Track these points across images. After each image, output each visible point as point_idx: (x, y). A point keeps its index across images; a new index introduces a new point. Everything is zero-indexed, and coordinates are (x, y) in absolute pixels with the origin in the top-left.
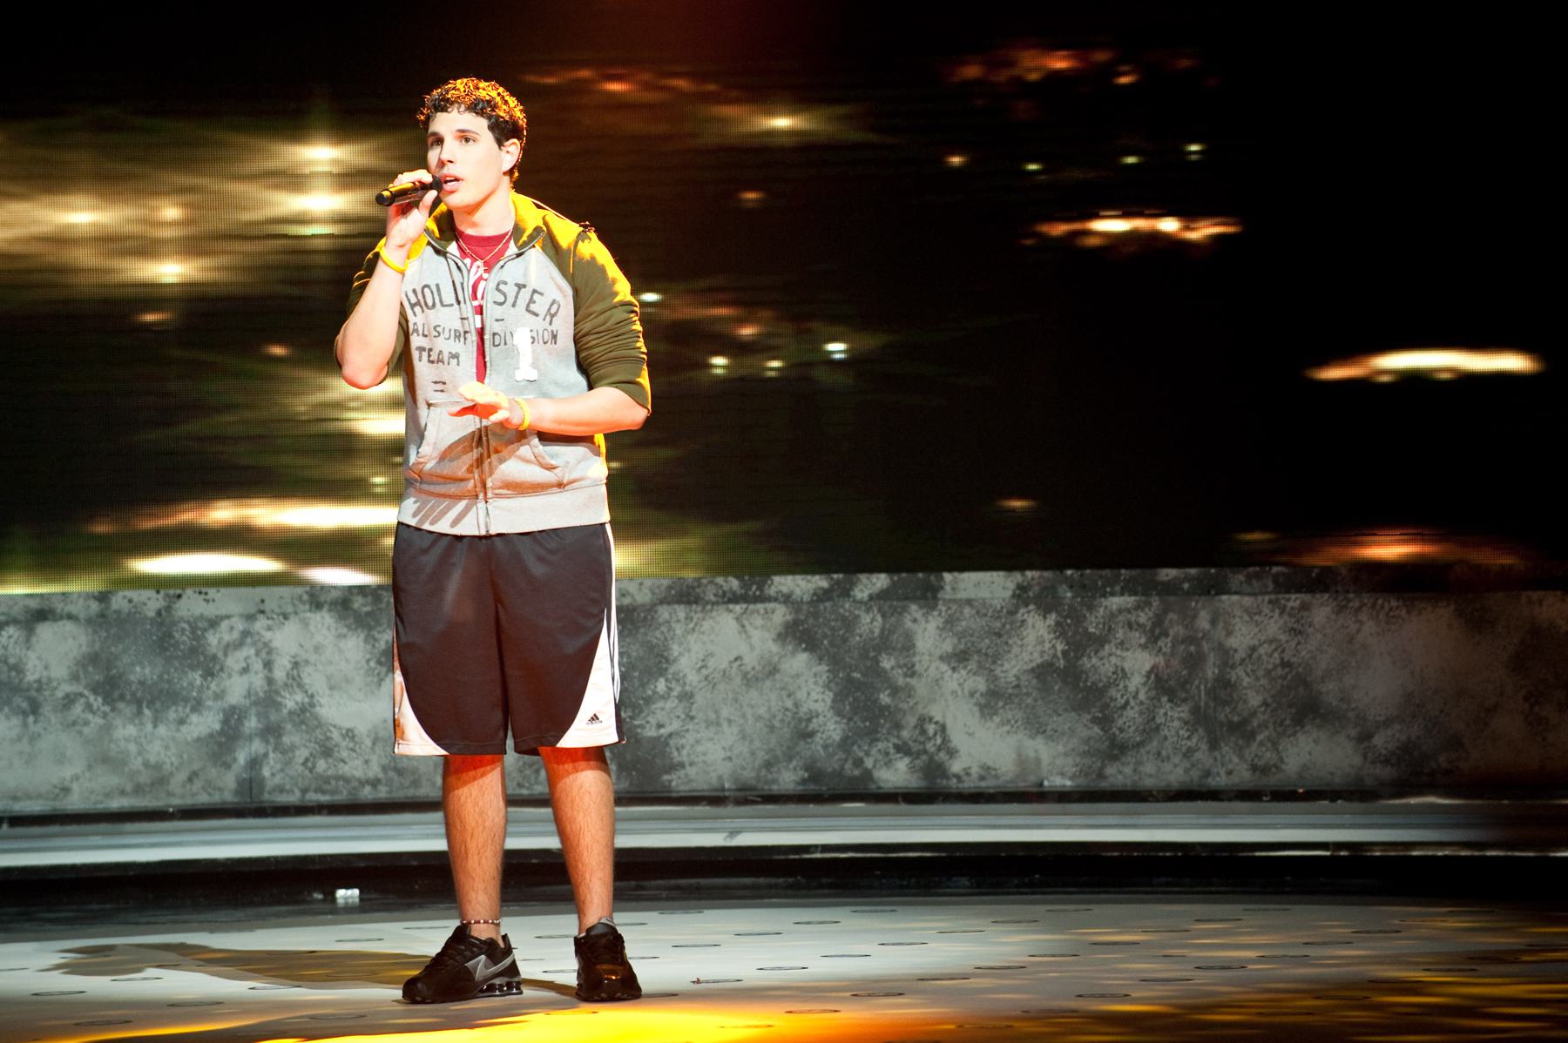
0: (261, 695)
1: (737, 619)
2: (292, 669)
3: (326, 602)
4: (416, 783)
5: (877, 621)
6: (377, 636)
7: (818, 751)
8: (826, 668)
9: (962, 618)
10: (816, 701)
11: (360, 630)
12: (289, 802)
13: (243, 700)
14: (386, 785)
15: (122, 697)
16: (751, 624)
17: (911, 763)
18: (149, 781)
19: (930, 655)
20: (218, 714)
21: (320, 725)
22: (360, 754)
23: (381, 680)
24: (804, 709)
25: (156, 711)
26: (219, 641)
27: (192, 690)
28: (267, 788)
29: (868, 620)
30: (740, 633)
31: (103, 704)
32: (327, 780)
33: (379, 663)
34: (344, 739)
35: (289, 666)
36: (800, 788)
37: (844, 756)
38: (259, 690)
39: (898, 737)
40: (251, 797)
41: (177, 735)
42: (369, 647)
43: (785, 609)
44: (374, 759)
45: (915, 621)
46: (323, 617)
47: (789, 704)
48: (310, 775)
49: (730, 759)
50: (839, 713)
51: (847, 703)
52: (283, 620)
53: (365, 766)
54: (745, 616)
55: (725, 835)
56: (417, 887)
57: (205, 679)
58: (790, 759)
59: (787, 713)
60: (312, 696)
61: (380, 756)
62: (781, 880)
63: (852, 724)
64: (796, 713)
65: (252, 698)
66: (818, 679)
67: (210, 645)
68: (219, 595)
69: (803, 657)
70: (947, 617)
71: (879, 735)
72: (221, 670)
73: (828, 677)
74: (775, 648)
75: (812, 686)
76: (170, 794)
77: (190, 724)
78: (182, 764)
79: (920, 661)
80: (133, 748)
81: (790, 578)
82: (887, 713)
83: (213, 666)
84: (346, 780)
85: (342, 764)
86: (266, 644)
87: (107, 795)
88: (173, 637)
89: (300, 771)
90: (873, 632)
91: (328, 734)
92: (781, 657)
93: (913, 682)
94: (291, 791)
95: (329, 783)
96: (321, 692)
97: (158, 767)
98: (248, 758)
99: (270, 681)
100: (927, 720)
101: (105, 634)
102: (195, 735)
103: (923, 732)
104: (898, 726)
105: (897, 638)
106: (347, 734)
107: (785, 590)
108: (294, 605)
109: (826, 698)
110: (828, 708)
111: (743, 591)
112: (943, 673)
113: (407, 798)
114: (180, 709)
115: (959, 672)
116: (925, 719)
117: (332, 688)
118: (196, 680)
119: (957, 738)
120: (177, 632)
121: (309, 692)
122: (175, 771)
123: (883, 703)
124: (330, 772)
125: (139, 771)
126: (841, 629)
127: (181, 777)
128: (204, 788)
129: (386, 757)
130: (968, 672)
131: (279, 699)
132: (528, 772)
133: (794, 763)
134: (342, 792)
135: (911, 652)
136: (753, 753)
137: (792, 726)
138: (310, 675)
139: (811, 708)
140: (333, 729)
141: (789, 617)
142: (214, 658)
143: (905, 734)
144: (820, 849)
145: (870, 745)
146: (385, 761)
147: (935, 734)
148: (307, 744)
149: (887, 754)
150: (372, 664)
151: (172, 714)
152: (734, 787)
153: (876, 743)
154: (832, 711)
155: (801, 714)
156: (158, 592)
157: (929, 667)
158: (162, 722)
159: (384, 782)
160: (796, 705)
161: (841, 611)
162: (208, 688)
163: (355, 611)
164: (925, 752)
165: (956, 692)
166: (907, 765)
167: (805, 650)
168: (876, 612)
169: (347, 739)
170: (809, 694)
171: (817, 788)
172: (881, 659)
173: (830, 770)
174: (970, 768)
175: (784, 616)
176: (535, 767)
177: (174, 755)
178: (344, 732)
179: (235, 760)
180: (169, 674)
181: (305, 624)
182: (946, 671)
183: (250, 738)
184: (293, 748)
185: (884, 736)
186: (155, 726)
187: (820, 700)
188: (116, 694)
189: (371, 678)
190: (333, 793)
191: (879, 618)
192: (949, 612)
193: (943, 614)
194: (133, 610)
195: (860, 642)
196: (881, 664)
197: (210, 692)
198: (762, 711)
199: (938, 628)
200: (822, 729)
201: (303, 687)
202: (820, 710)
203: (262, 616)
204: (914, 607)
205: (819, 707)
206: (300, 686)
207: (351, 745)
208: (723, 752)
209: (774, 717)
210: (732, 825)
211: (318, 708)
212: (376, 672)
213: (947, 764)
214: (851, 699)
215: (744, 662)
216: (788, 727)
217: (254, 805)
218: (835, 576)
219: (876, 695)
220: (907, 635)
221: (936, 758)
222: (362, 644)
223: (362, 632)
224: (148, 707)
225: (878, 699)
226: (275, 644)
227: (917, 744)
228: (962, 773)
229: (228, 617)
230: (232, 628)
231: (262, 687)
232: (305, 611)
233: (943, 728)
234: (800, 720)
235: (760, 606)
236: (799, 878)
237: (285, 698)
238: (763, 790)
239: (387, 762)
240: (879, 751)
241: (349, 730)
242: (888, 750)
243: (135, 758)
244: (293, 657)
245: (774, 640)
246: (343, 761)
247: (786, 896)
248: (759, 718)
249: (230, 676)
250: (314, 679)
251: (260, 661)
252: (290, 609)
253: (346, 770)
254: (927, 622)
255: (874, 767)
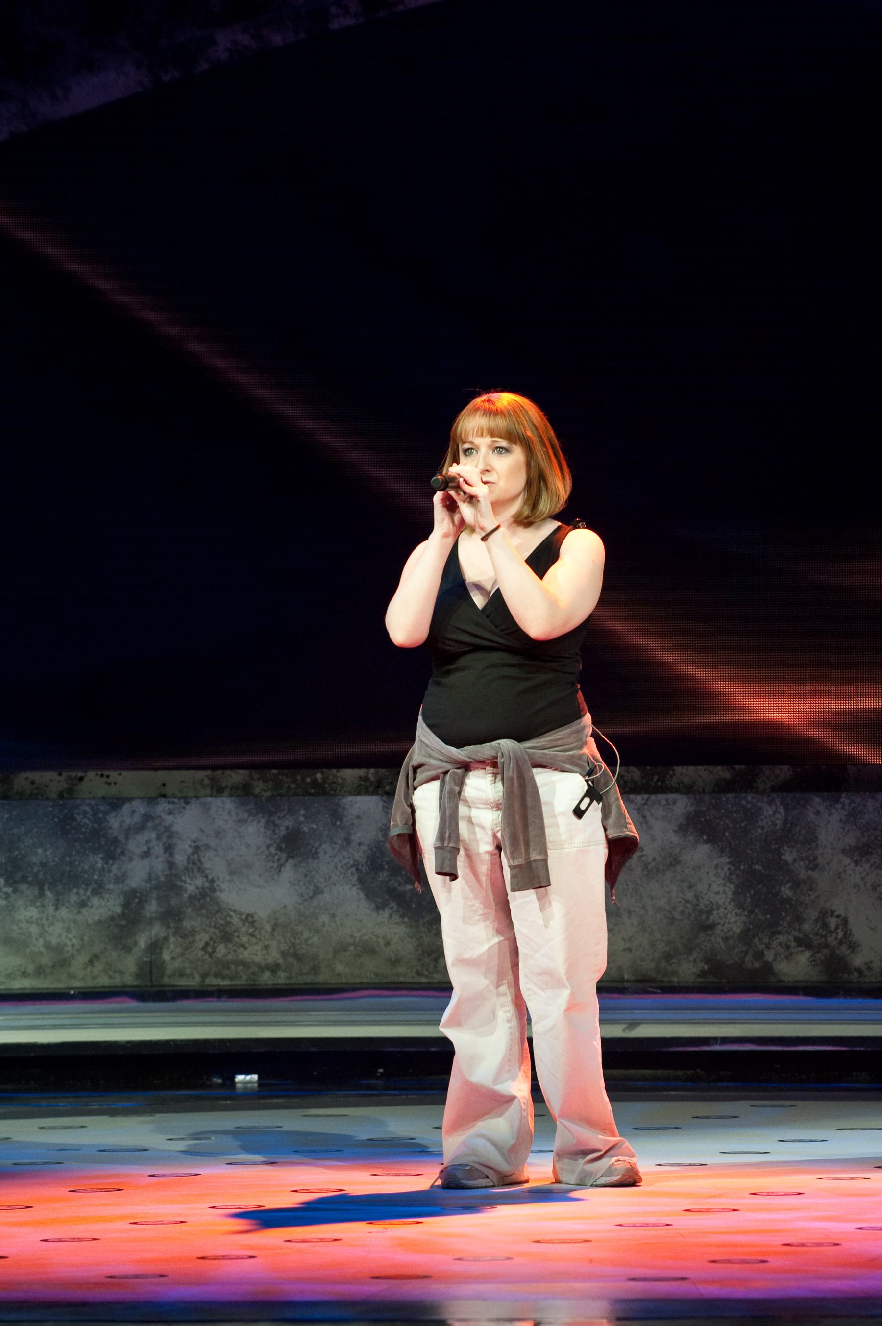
0: (162, 878)
1: (638, 809)
2: (193, 853)
3: (227, 787)
4: (315, 969)
5: (779, 813)
6: (277, 822)
7: (719, 943)
8: (728, 860)
9: (866, 811)
10: (718, 893)
11: (261, 815)
12: (188, 986)
13: (144, 884)
14: (285, 971)
15: (24, 879)
16: (652, 815)
17: (811, 956)
18: (50, 964)
19: (833, 848)
20: (119, 897)
21: (220, 910)
22: (260, 940)
23: (281, 866)
24: (704, 902)
25: (58, 894)
26: (121, 826)
27: (94, 874)
28: (168, 972)
29: (771, 813)
30: (641, 824)
31: (5, 886)
32: (227, 965)
33: (280, 849)
34: (244, 925)
35: (190, 851)
36: (701, 980)
37: (744, 949)
38: (160, 874)
39: (800, 930)
40: (151, 982)
41: (79, 917)
42: (270, 832)
43: (687, 800)
44: (275, 943)
45: (818, 813)
46: (223, 801)
47: (689, 895)
48: (209, 959)
49: (630, 950)
50: (740, 906)
51: (748, 895)
52: (184, 805)
53: (265, 952)
54: (646, 807)
55: (624, 1026)
56: (315, 1073)
57: (107, 863)
58: (690, 951)
59: (688, 905)
60: (212, 881)
61: (279, 942)
62: (680, 1073)
63: (752, 916)
64: (697, 905)
65: (153, 882)
66: (720, 871)
67: (111, 828)
68: (121, 777)
69: (704, 849)
70: (850, 810)
71: (780, 928)
72: (123, 853)
73: (729, 869)
74: (676, 839)
75: (713, 879)
76: (71, 976)
77: (92, 907)
78: (83, 946)
79: (822, 854)
80: (34, 929)
81: (692, 768)
82: (788, 906)
83: (115, 849)
84: (245, 965)
85: (242, 949)
86: (167, 829)
87: (8, 976)
88: (74, 819)
89: (200, 955)
90: (776, 825)
91: (228, 919)
92: (682, 849)
93: (815, 875)
94: (191, 975)
95: (229, 968)
96: (221, 877)
97: (59, 949)
98: (149, 942)
99: (171, 865)
100: (829, 913)
101: (7, 816)
102: (96, 918)
103: (825, 925)
104: (799, 919)
105: (800, 831)
106: (247, 918)
107: (686, 780)
108: (195, 789)
109: (727, 890)
110: (728, 900)
111: (644, 781)
112: (845, 866)
113: (306, 984)
114: (82, 891)
115: (862, 866)
116: (827, 912)
117: (232, 873)
118: (96, 862)
119: (859, 931)
120: (78, 814)
121: (210, 877)
122: (76, 953)
123: (785, 896)
124: (230, 957)
125: (41, 953)
126: (742, 821)
127: (83, 959)
128: (104, 971)
129: (286, 942)
130: (871, 866)
131: (179, 883)
132: (427, 960)
133: (695, 955)
134: (241, 977)
135: (814, 844)
136: (653, 945)
137: (692, 919)
138: (210, 860)
139: (712, 899)
140: (232, 914)
141: (691, 809)
142: (115, 841)
143: (806, 927)
144: (719, 1042)
145: (770, 938)
146: (284, 947)
147: (837, 928)
148: (208, 929)
149: (788, 947)
150: (273, 850)
151: (73, 898)
152: (633, 978)
153: (777, 936)
154: (732, 903)
155: (702, 907)
156: (60, 774)
157: (832, 859)
158: (63, 905)
159: (283, 967)
160: (697, 897)
161: (743, 802)
162: (110, 871)
163: (255, 796)
164: (827, 945)
165: (858, 886)
166: (808, 959)
167: (706, 842)
168: (778, 803)
169: (247, 924)
170: (710, 886)
171: (715, 980)
172: (783, 852)
173: (731, 962)
174: (871, 962)
175: (685, 808)
176: (434, 955)
177: (74, 937)
178: (244, 917)
179: (136, 943)
180: (70, 856)
181: (207, 808)
182: (849, 864)
183: (151, 922)
184: (193, 932)
185: (785, 929)
186: (57, 909)
187: (721, 891)
188: (19, 875)
189: (271, 864)
190: (232, 978)
191: (782, 810)
192: (853, 805)
193: (847, 807)
194: (35, 792)
195: (762, 834)
196: (783, 856)
197: (112, 875)
198: (662, 902)
199: (841, 820)
200: (722, 922)
201: (203, 872)
202: (720, 902)
203: (163, 800)
204: (817, 800)
205: (720, 899)
206: (201, 870)
207: (251, 930)
208: (623, 942)
209: (674, 908)
210: (632, 1016)
211: (218, 893)
212: (276, 857)
213: (849, 958)
214: (752, 892)
215: (644, 853)
216: (689, 919)
217: (154, 989)
218: (738, 767)
219: (777, 887)
220: (810, 827)
221: (838, 952)
222: (262, 830)
223: (263, 817)
224: (49, 889)
225: (780, 891)
226: (176, 828)
227: (819, 937)
228: (864, 968)
229: (130, 799)
230: (134, 812)
231: (163, 871)
232: (206, 796)
233: (845, 921)
234: (701, 912)
235: (662, 797)
236: (698, 1070)
237: (185, 882)
238: (662, 981)
239: (287, 948)
240: (780, 944)
241: (248, 915)
242: (788, 943)
243: (37, 940)
244: (194, 842)
245: (675, 831)
246: (243, 946)
247: (685, 1089)
248: (660, 909)
249: (131, 859)
250: (216, 865)
251: (161, 845)
252: (191, 794)
253: (245, 955)
254: (830, 814)
255: (774, 960)
